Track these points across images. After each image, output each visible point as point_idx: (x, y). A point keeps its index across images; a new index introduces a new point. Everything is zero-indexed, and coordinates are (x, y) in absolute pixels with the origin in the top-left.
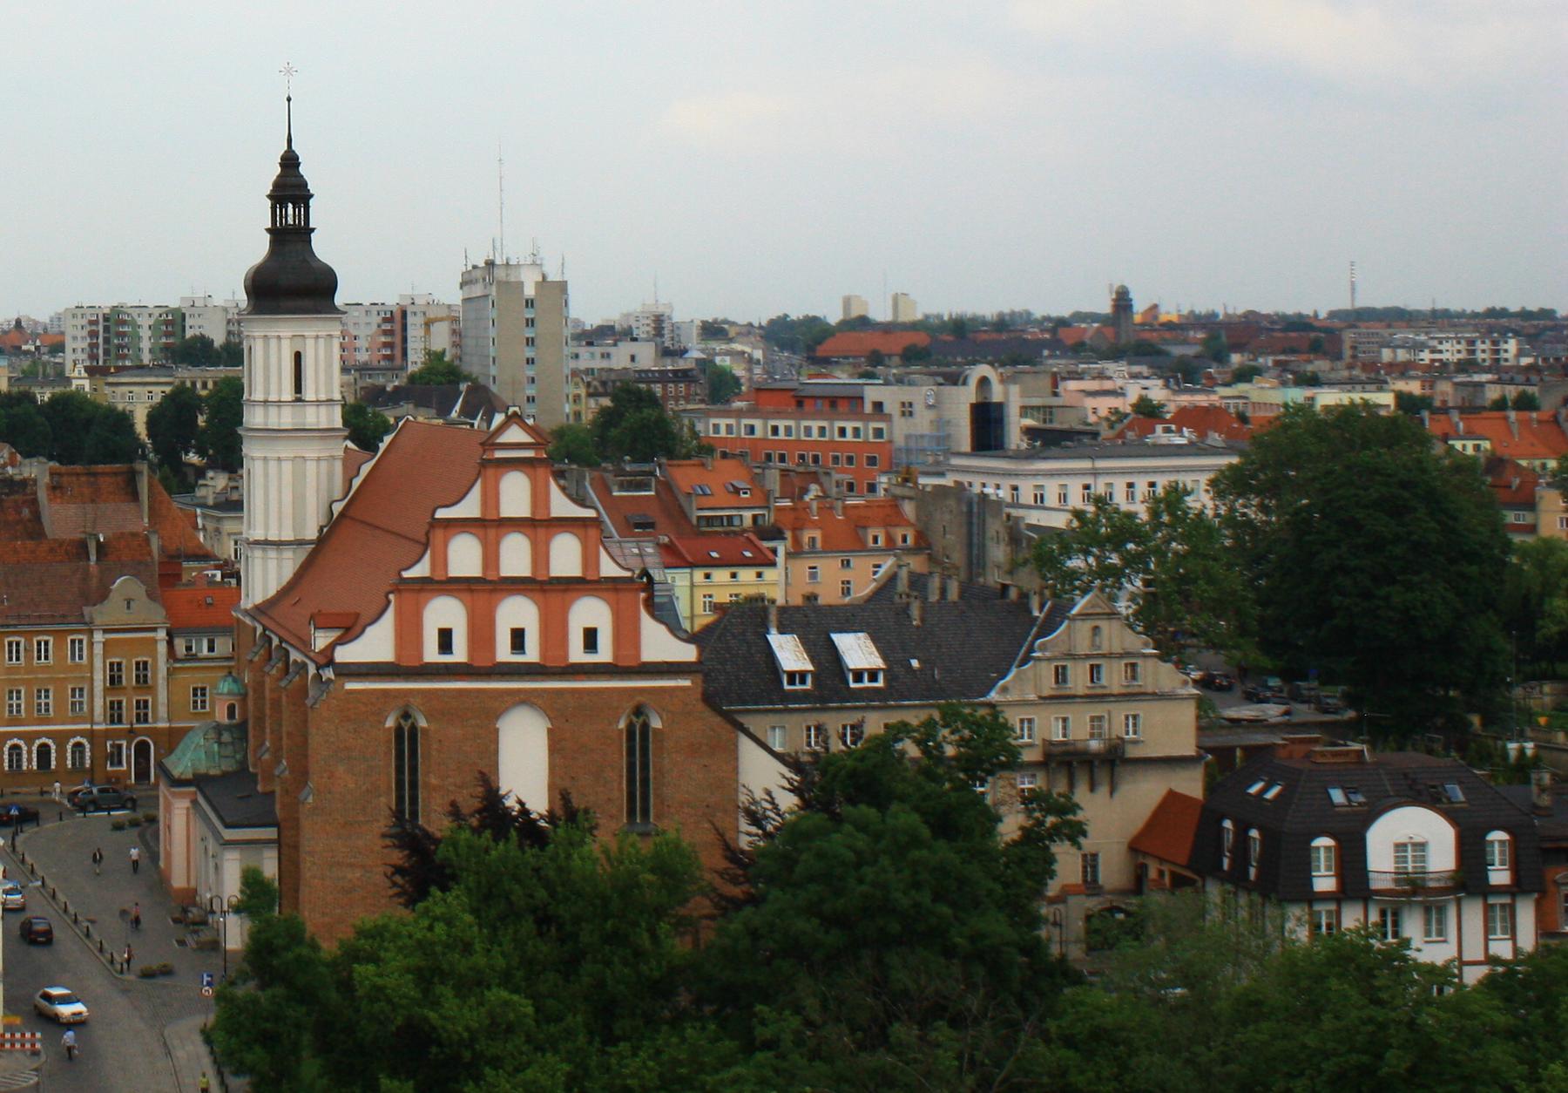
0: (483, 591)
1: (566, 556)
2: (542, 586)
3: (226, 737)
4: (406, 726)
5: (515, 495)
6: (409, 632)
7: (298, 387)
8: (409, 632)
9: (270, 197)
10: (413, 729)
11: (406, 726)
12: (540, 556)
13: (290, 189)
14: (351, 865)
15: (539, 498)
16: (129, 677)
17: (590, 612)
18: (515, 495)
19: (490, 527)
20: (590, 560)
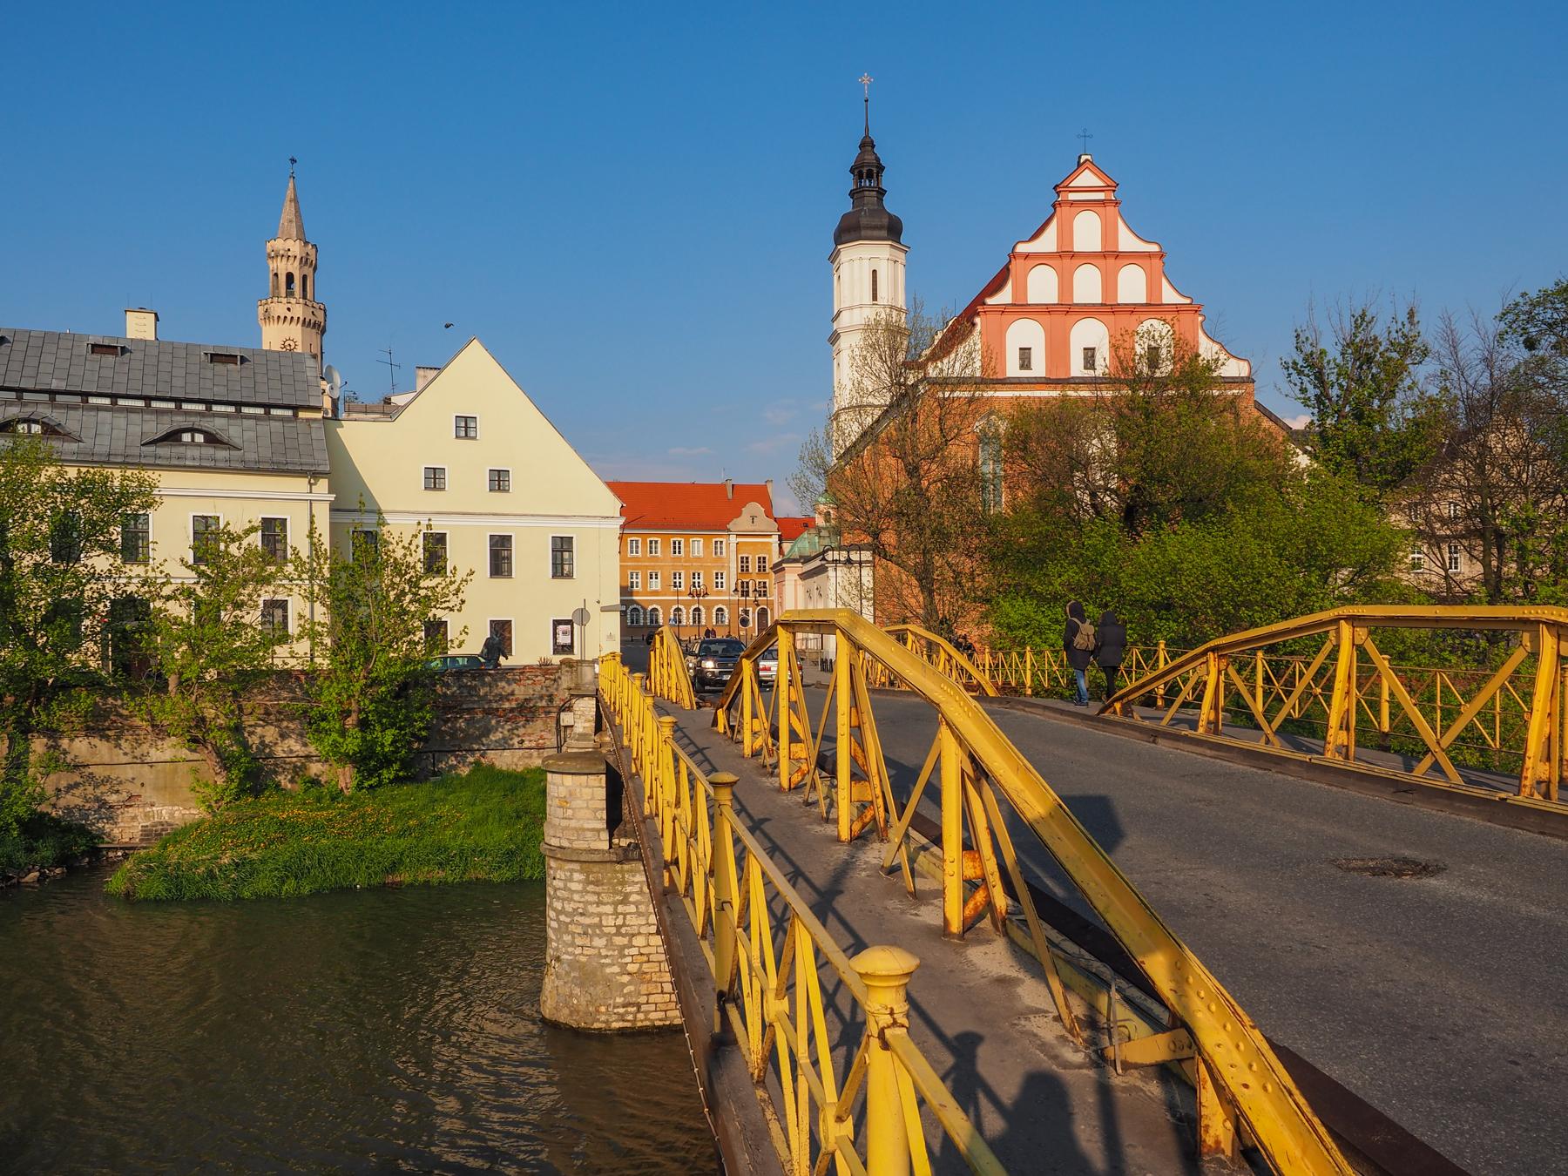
1: (1132, 285)
2: (1107, 309)
3: (824, 533)
5: (1087, 231)
7: (875, 297)
9: (852, 171)
12: (1109, 284)
15: (1109, 233)
16: (753, 567)
18: (1087, 231)
19: (1066, 257)
20: (1153, 287)
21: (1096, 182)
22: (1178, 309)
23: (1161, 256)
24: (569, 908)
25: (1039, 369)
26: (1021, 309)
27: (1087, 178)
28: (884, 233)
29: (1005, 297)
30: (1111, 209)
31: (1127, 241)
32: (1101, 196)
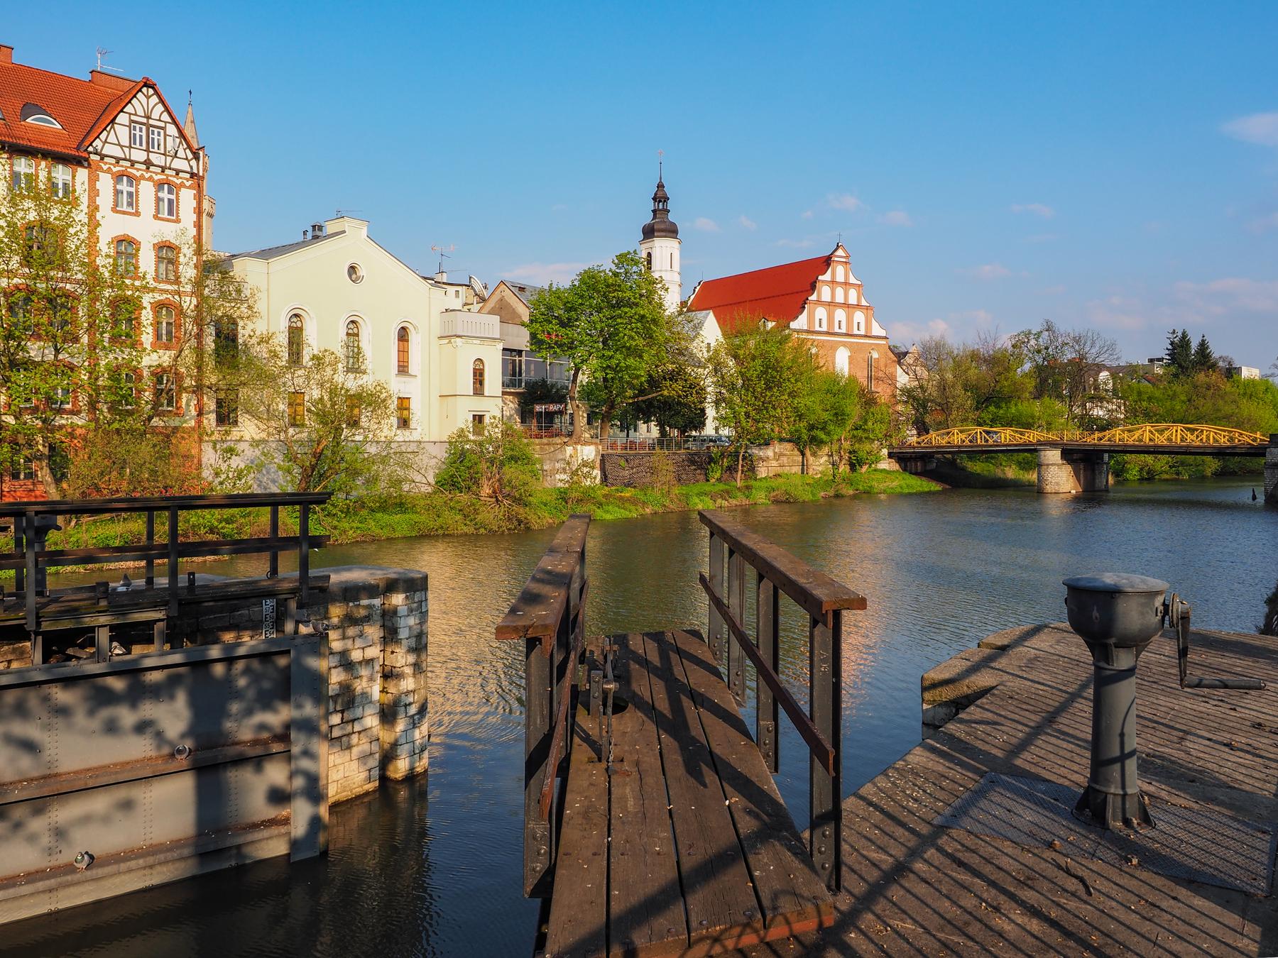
0: (832, 305)
1: (853, 298)
2: (846, 305)
13: (660, 197)
15: (846, 276)
26: (819, 302)
29: (813, 297)
31: (852, 280)
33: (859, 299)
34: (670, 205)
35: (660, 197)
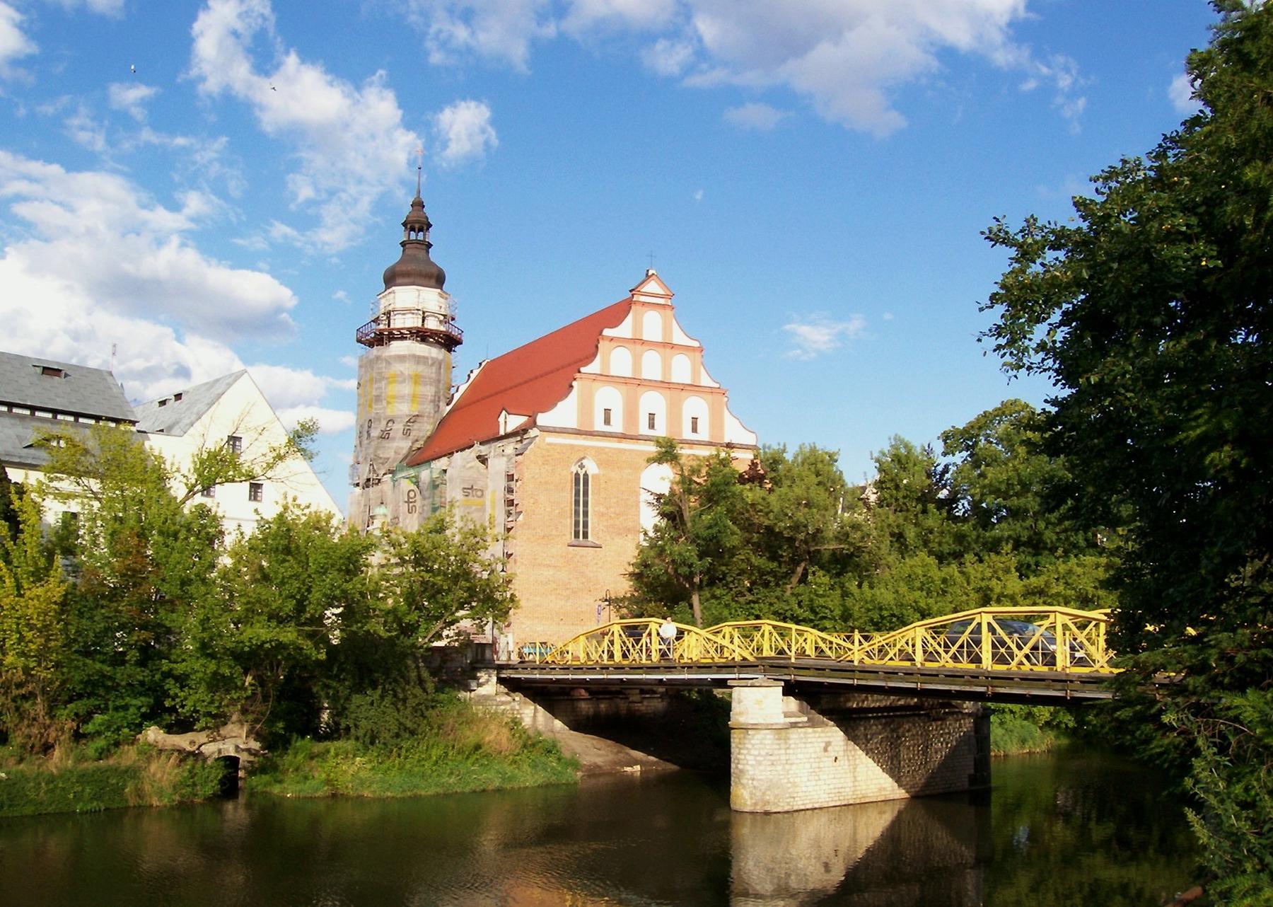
1: (682, 369)
2: (665, 385)
4: (582, 474)
6: (586, 408)
8: (586, 408)
10: (586, 475)
11: (582, 474)
13: (417, 224)
14: (548, 566)
15: (667, 329)
17: (695, 406)
21: (661, 292)
22: (711, 391)
23: (701, 349)
24: (763, 752)
25: (617, 426)
27: (652, 287)
28: (433, 282)
29: (594, 367)
30: (669, 312)
31: (679, 337)
32: (662, 301)
33: (695, 373)
34: (431, 236)
35: (417, 224)
